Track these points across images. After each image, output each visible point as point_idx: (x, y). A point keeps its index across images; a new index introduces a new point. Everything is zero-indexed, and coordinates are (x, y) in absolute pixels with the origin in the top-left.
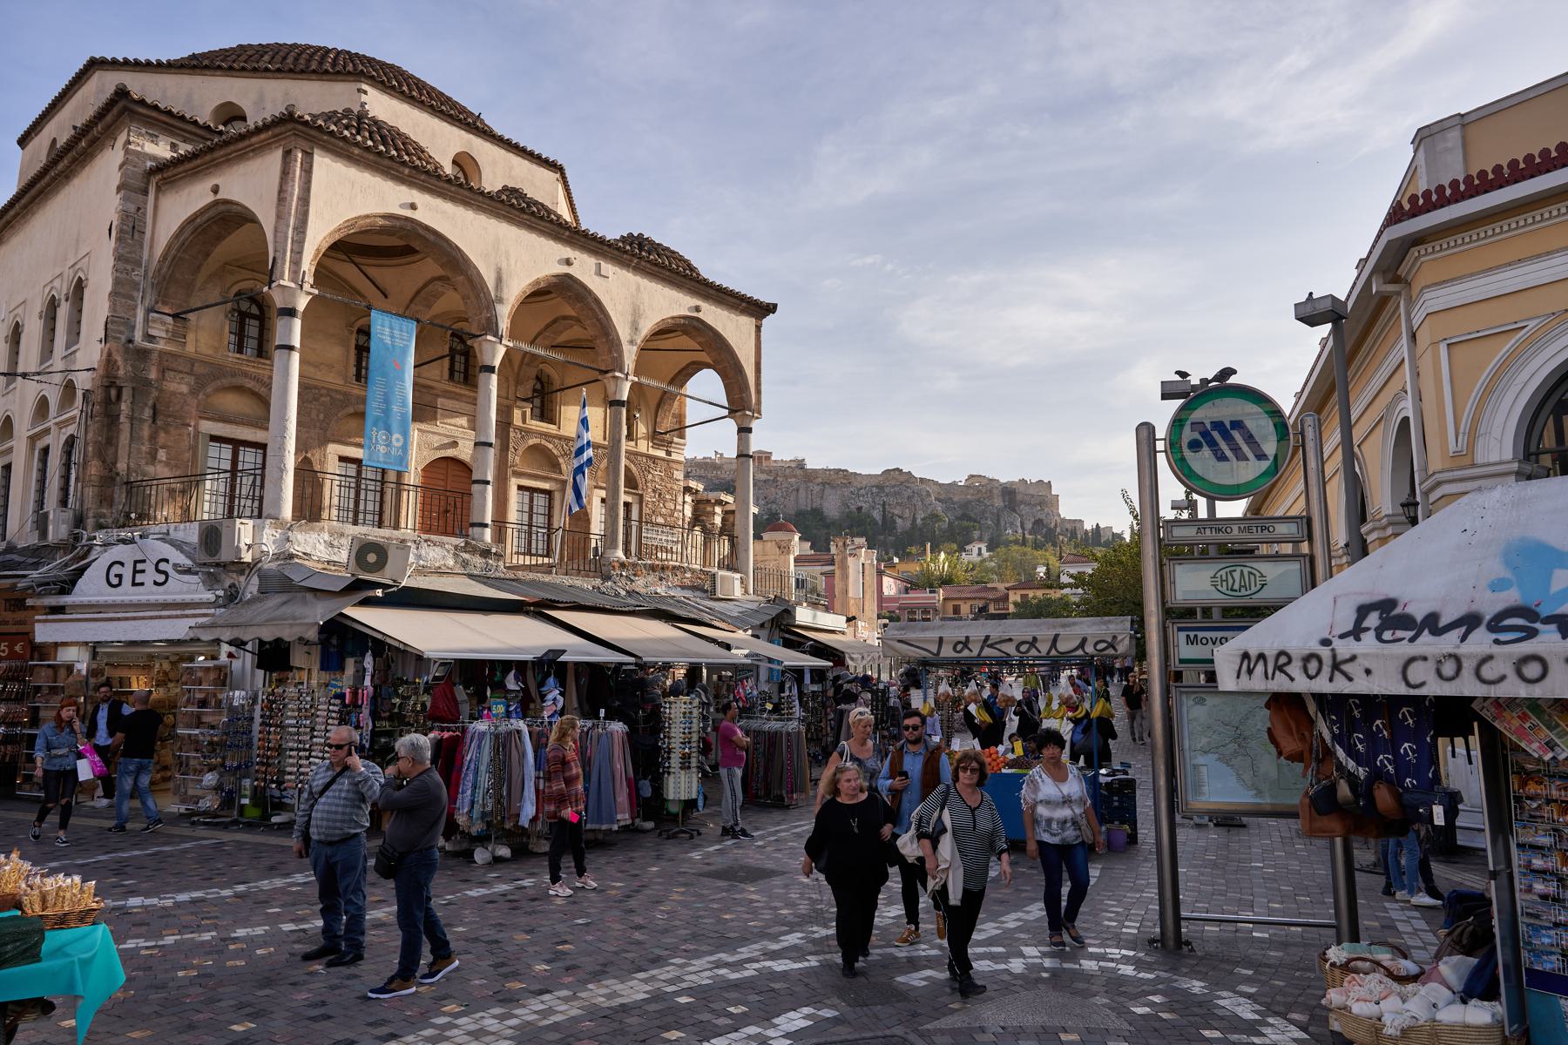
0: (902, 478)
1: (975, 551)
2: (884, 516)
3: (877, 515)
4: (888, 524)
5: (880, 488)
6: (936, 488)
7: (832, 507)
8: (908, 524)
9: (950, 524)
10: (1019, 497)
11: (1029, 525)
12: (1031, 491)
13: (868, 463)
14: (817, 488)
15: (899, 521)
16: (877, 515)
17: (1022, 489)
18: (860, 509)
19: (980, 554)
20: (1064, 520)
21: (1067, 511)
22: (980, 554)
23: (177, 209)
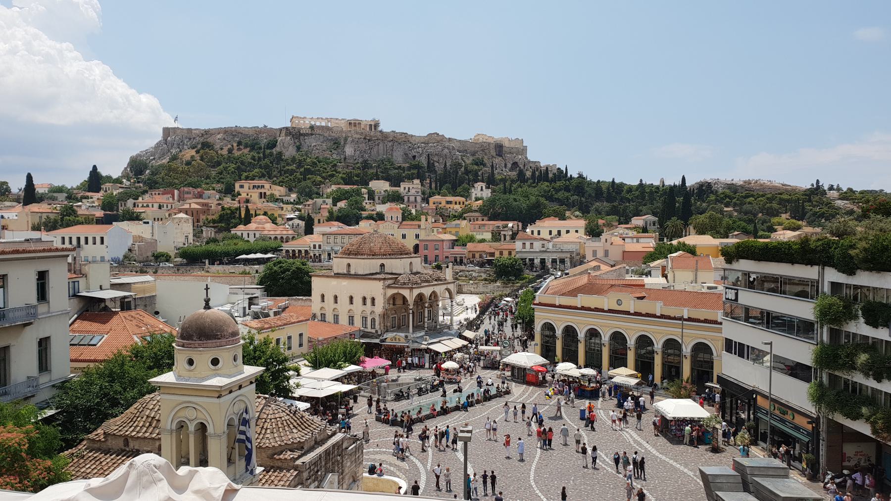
0: (439, 138)
1: (479, 188)
2: (429, 162)
3: (424, 161)
4: (431, 167)
5: (426, 143)
6: (458, 144)
7: (398, 158)
8: (442, 166)
9: (466, 168)
10: (504, 149)
11: (509, 165)
12: (512, 145)
13: (418, 129)
14: (390, 144)
15: (436, 164)
16: (424, 161)
17: (506, 144)
18: (414, 157)
19: (482, 190)
20: (529, 162)
21: (532, 156)
22: (482, 190)
23: (391, 292)
